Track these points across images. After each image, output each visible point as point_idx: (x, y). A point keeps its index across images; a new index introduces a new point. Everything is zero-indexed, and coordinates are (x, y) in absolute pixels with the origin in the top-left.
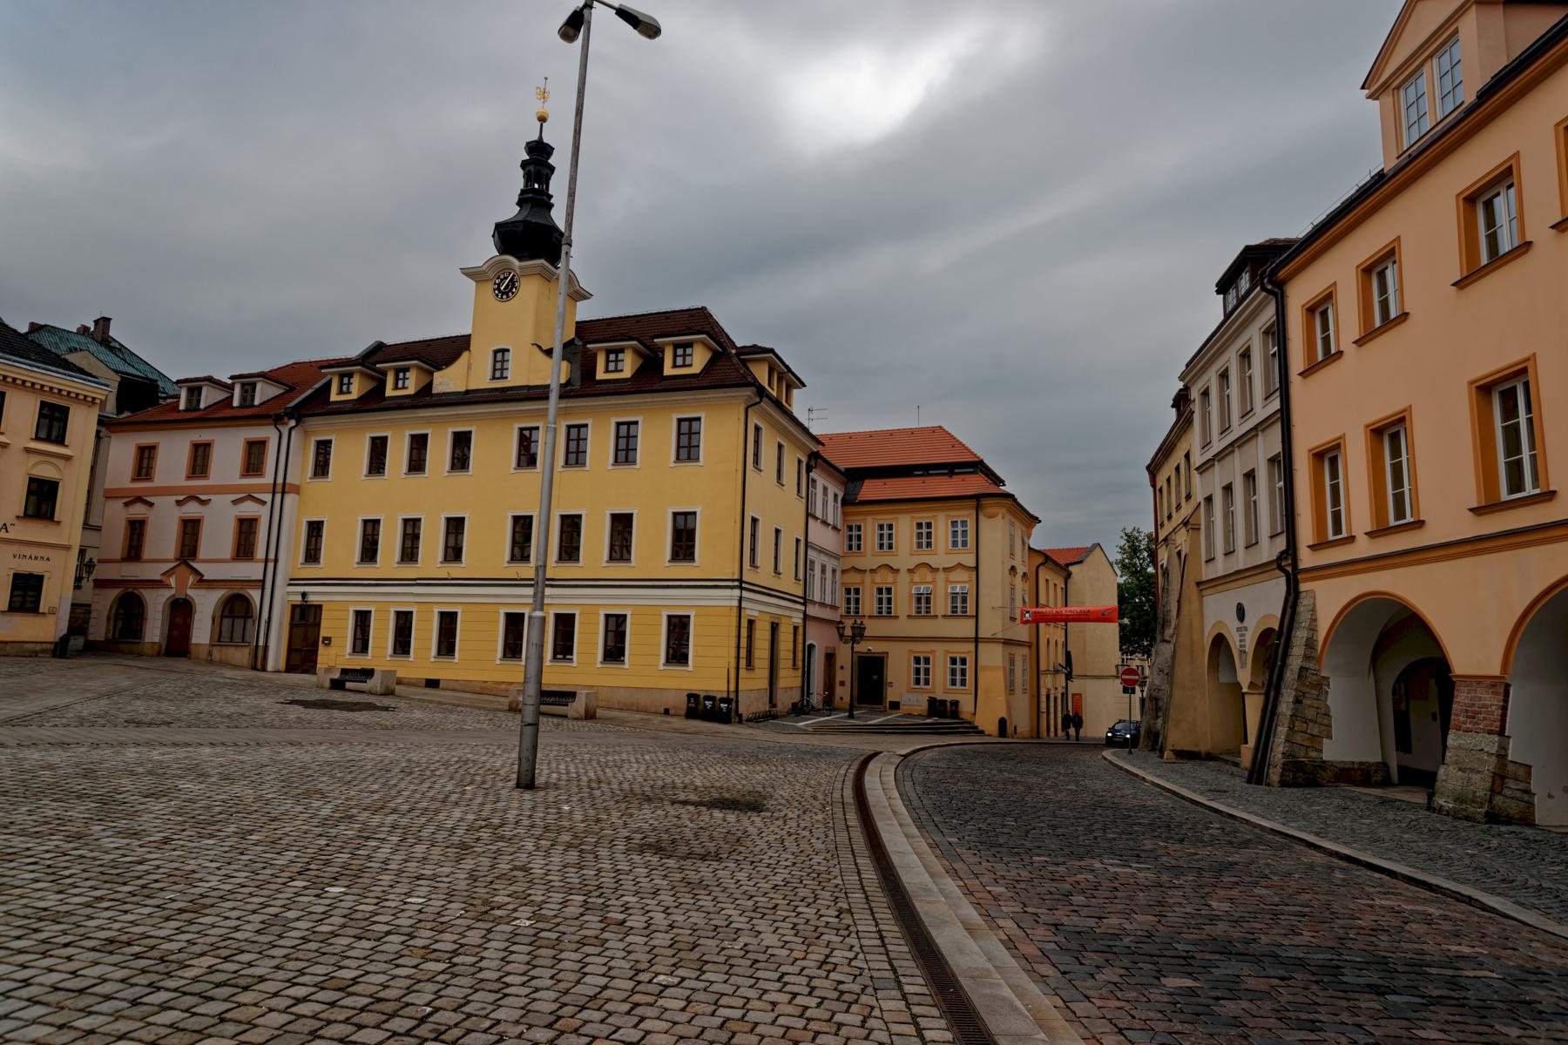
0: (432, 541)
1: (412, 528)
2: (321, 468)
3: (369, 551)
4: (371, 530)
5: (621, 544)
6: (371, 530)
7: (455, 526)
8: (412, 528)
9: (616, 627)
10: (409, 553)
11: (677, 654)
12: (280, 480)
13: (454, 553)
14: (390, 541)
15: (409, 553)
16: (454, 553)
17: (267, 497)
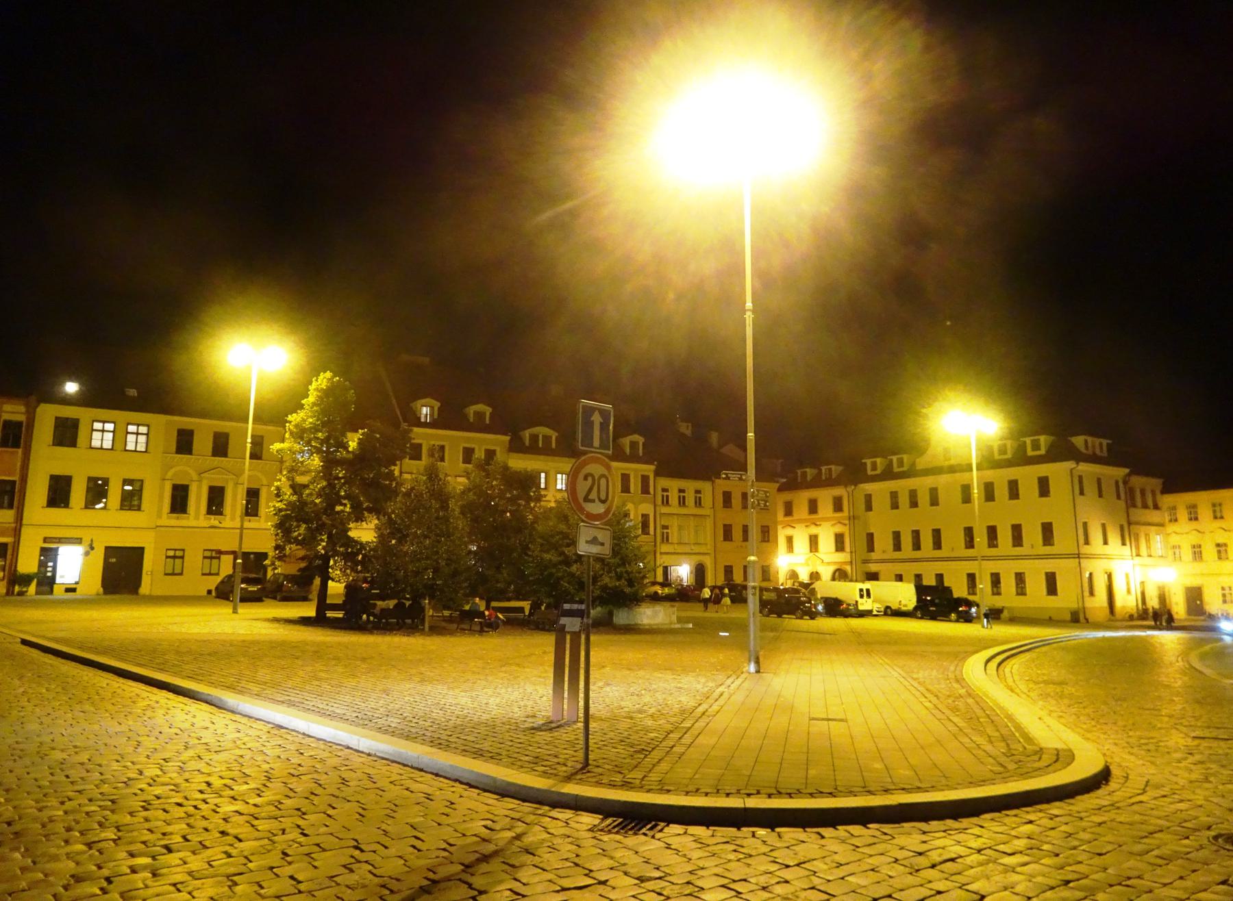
0: (927, 540)
1: (916, 535)
2: (869, 508)
3: (897, 547)
4: (897, 536)
5: (1017, 539)
6: (897, 536)
7: (937, 534)
8: (916, 535)
9: (1020, 578)
10: (917, 546)
11: (1052, 589)
12: (851, 514)
13: (937, 545)
14: (906, 541)
15: (917, 546)
16: (937, 545)
17: (847, 522)
